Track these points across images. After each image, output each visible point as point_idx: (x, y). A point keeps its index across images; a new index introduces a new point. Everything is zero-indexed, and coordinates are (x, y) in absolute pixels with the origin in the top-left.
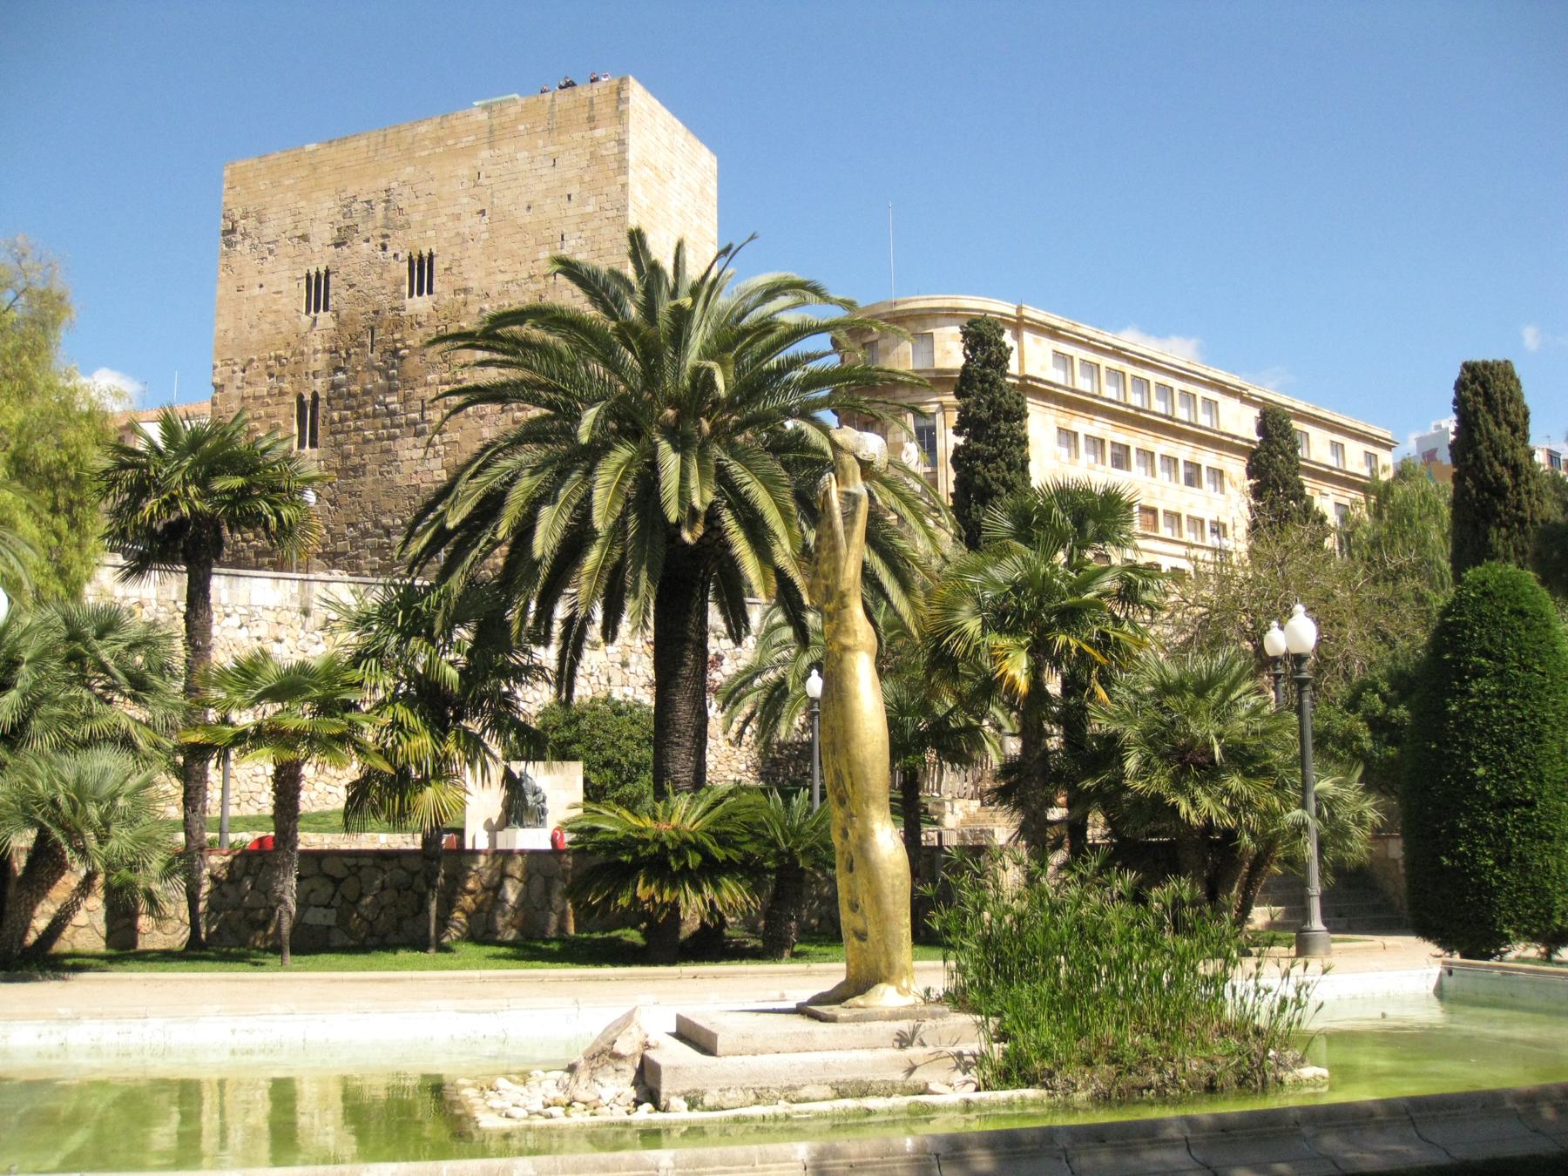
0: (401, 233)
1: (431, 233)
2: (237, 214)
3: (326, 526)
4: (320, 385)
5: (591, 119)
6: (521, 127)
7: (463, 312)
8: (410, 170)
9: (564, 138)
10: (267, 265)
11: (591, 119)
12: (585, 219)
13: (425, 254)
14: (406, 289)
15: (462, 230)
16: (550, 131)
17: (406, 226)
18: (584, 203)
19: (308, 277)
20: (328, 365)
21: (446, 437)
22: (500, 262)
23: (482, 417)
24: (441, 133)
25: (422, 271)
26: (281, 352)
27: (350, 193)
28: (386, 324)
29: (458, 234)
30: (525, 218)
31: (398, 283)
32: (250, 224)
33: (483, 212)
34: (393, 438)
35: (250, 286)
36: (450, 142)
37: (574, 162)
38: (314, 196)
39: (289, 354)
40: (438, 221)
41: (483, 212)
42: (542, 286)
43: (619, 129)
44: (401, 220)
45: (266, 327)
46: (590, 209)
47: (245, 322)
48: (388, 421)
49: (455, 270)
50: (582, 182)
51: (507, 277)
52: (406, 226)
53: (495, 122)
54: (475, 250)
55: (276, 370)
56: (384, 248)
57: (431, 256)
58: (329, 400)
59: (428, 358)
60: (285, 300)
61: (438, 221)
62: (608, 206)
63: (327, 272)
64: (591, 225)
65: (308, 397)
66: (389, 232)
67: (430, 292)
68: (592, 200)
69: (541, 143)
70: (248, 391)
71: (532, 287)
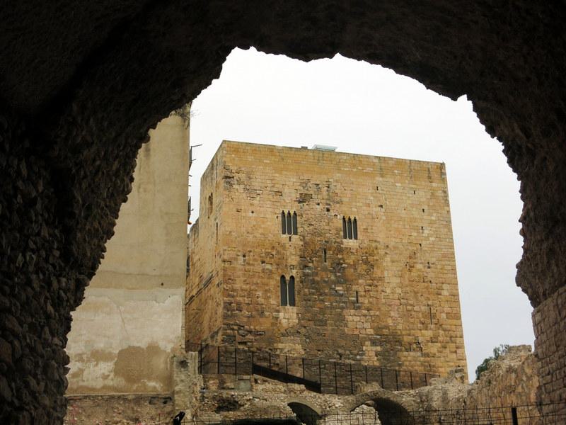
0: (338, 205)
1: (355, 210)
2: (234, 169)
4: (294, 273)
5: (429, 177)
6: (396, 171)
7: (375, 252)
8: (338, 175)
10: (255, 202)
11: (429, 177)
12: (432, 223)
13: (352, 219)
14: (342, 233)
15: (371, 212)
16: (411, 178)
17: (340, 202)
18: (430, 215)
20: (300, 264)
21: (372, 313)
22: (392, 232)
25: (350, 228)
26: (270, 251)
27: (306, 177)
28: (333, 249)
31: (338, 230)
32: (243, 176)
33: (381, 206)
34: (342, 308)
36: (360, 168)
37: (422, 195)
38: (284, 173)
39: (274, 253)
41: (381, 206)
43: (443, 185)
45: (258, 235)
46: (433, 218)
47: (243, 230)
48: (338, 298)
50: (429, 206)
51: (398, 240)
52: (340, 202)
53: (383, 165)
55: (267, 260)
56: (328, 210)
57: (355, 220)
58: (302, 282)
60: (269, 223)
62: (442, 219)
63: (295, 214)
64: (435, 226)
65: (288, 278)
66: (331, 203)
67: (356, 238)
68: (435, 214)
69: (407, 181)
70: (247, 267)
71: (410, 248)
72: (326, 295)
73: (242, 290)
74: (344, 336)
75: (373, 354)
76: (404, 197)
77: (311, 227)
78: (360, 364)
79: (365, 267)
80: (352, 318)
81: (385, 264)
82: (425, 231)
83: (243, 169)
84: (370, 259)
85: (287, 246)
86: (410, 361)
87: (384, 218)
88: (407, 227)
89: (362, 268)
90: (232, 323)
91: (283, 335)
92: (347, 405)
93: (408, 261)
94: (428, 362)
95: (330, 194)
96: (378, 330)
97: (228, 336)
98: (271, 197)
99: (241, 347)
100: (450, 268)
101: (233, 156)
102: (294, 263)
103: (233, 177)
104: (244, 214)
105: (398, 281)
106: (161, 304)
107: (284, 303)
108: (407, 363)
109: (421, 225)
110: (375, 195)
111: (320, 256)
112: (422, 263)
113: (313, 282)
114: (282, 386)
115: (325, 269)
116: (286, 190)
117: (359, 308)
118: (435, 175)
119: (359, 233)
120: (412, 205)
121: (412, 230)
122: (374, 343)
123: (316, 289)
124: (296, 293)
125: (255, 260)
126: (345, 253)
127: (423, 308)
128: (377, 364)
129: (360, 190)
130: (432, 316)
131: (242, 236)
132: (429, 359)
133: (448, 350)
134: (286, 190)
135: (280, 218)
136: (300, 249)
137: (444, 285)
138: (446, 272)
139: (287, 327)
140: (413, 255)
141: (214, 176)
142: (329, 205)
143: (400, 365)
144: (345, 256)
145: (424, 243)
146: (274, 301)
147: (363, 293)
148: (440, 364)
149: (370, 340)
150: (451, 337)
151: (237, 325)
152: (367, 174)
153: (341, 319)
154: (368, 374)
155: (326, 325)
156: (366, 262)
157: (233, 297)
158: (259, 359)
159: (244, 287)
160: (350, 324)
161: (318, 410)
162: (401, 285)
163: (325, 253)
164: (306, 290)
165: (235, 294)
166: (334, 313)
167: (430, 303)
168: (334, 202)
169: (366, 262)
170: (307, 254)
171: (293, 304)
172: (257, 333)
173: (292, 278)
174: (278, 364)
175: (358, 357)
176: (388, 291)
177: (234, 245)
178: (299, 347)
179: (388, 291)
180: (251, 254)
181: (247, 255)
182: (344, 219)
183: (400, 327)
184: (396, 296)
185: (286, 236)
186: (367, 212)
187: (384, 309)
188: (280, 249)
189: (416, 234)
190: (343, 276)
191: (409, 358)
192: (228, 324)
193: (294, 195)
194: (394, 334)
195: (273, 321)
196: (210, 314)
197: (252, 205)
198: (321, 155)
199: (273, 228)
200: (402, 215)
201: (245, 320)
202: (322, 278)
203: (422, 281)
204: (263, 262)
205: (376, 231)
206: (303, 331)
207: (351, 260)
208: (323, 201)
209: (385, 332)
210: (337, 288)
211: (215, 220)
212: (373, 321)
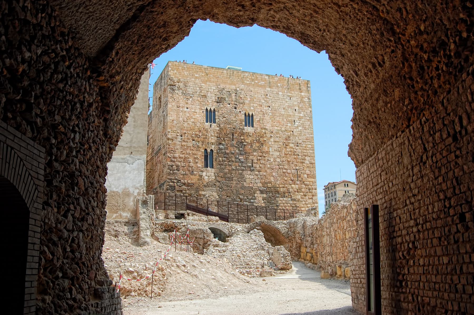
2: (176, 80)
3: (219, 196)
5: (300, 89)
6: (279, 85)
7: (265, 135)
9: (293, 92)
10: (189, 102)
11: (300, 89)
12: (300, 118)
13: (251, 114)
14: (244, 123)
15: (263, 110)
16: (288, 89)
18: (300, 113)
19: (207, 109)
20: (217, 142)
21: (261, 173)
22: (275, 123)
23: (272, 169)
24: (253, 78)
25: (249, 120)
27: (222, 86)
29: (261, 111)
30: (283, 112)
32: (181, 85)
34: (243, 170)
35: (183, 107)
38: (208, 83)
39: (200, 134)
40: (255, 105)
42: (289, 134)
44: (242, 101)
45: (190, 123)
46: (301, 115)
47: (181, 119)
48: (240, 164)
49: (261, 122)
51: (279, 128)
52: (243, 103)
54: (267, 118)
55: (196, 139)
56: (235, 108)
57: (252, 115)
58: (218, 153)
59: (254, 147)
61: (255, 105)
62: (307, 115)
63: (214, 110)
64: (302, 120)
66: (237, 104)
67: (253, 126)
68: (302, 113)
70: (183, 143)
72: (233, 162)
73: (180, 158)
74: (243, 187)
75: (261, 199)
76: (283, 102)
77: (224, 119)
78: (253, 205)
79: (257, 145)
80: (248, 176)
81: (270, 143)
82: (297, 123)
83: (182, 80)
84: (261, 139)
85: (209, 130)
86: (284, 203)
87: (270, 114)
88: (285, 120)
89: (255, 146)
90: (173, 178)
91: (205, 186)
92: (245, 229)
93: (285, 141)
94: (295, 204)
95: (237, 98)
96: (264, 184)
97: (171, 186)
98: (199, 99)
99: (178, 194)
100: (310, 146)
101: (175, 71)
102: (213, 141)
103: (175, 85)
104: (181, 109)
105: (278, 154)
106: (131, 165)
107: (206, 166)
108: (282, 205)
109: (293, 119)
110: (265, 99)
111: (230, 138)
112: (293, 143)
113: (226, 153)
114: (204, 217)
115: (232, 146)
116: (209, 94)
117: (253, 170)
118: (304, 88)
119: (254, 123)
120: (289, 107)
121: (288, 122)
122: (262, 192)
123: (227, 158)
124: (214, 160)
125: (188, 139)
126: (245, 135)
127: (293, 171)
128: (263, 205)
129: (256, 96)
130: (299, 176)
131: (180, 123)
132: (295, 202)
133: (307, 197)
134: (209, 95)
135: (205, 113)
136: (217, 133)
137: (306, 157)
138: (308, 149)
139: (208, 181)
140: (288, 138)
141: (163, 84)
142: (236, 105)
143: (277, 206)
144: (245, 138)
145: (295, 130)
146: (200, 164)
147: (256, 161)
148: (303, 206)
149: (260, 190)
150: (309, 189)
151: (176, 179)
152: (261, 86)
153: (242, 177)
154: (258, 211)
155: (232, 180)
156: (259, 141)
157: (174, 162)
158: (190, 201)
159: (181, 156)
160: (247, 180)
161: (226, 231)
162: (279, 157)
163: (233, 135)
164: (220, 158)
165: (175, 160)
166: (237, 173)
167: (297, 168)
168: (239, 103)
169: (259, 141)
170: (221, 137)
171: (212, 167)
172: (188, 185)
173: (212, 150)
174: (202, 204)
175: (252, 201)
176: (272, 160)
177: (175, 129)
178: (215, 194)
179: (272, 160)
180: (186, 135)
181: (183, 135)
182: (245, 114)
183: (278, 182)
184: (277, 163)
185: (208, 124)
186: (259, 110)
187: (268, 171)
188: (205, 132)
189: (290, 125)
190: (244, 150)
191: (283, 202)
192: (171, 179)
193: (214, 98)
194: (275, 187)
195: (198, 177)
196: (158, 172)
197: (187, 103)
198: (232, 73)
199: (200, 118)
200: (282, 113)
201: (182, 176)
202: (231, 151)
203: (293, 154)
204: (193, 140)
205: (266, 123)
206: (218, 184)
207: (249, 141)
208: (232, 102)
209: (269, 185)
210: (240, 158)
211: (163, 112)
212: (261, 179)
